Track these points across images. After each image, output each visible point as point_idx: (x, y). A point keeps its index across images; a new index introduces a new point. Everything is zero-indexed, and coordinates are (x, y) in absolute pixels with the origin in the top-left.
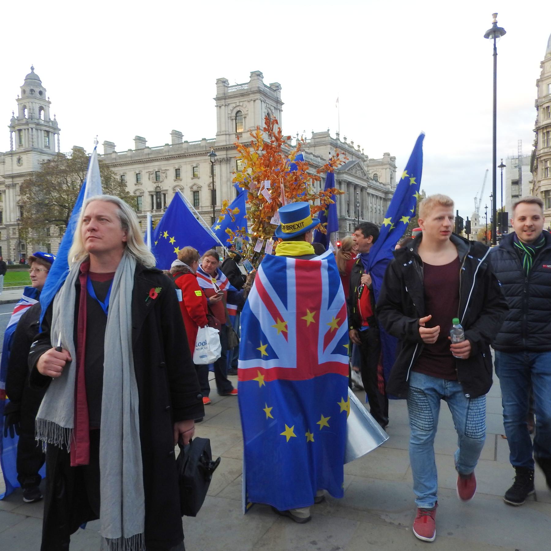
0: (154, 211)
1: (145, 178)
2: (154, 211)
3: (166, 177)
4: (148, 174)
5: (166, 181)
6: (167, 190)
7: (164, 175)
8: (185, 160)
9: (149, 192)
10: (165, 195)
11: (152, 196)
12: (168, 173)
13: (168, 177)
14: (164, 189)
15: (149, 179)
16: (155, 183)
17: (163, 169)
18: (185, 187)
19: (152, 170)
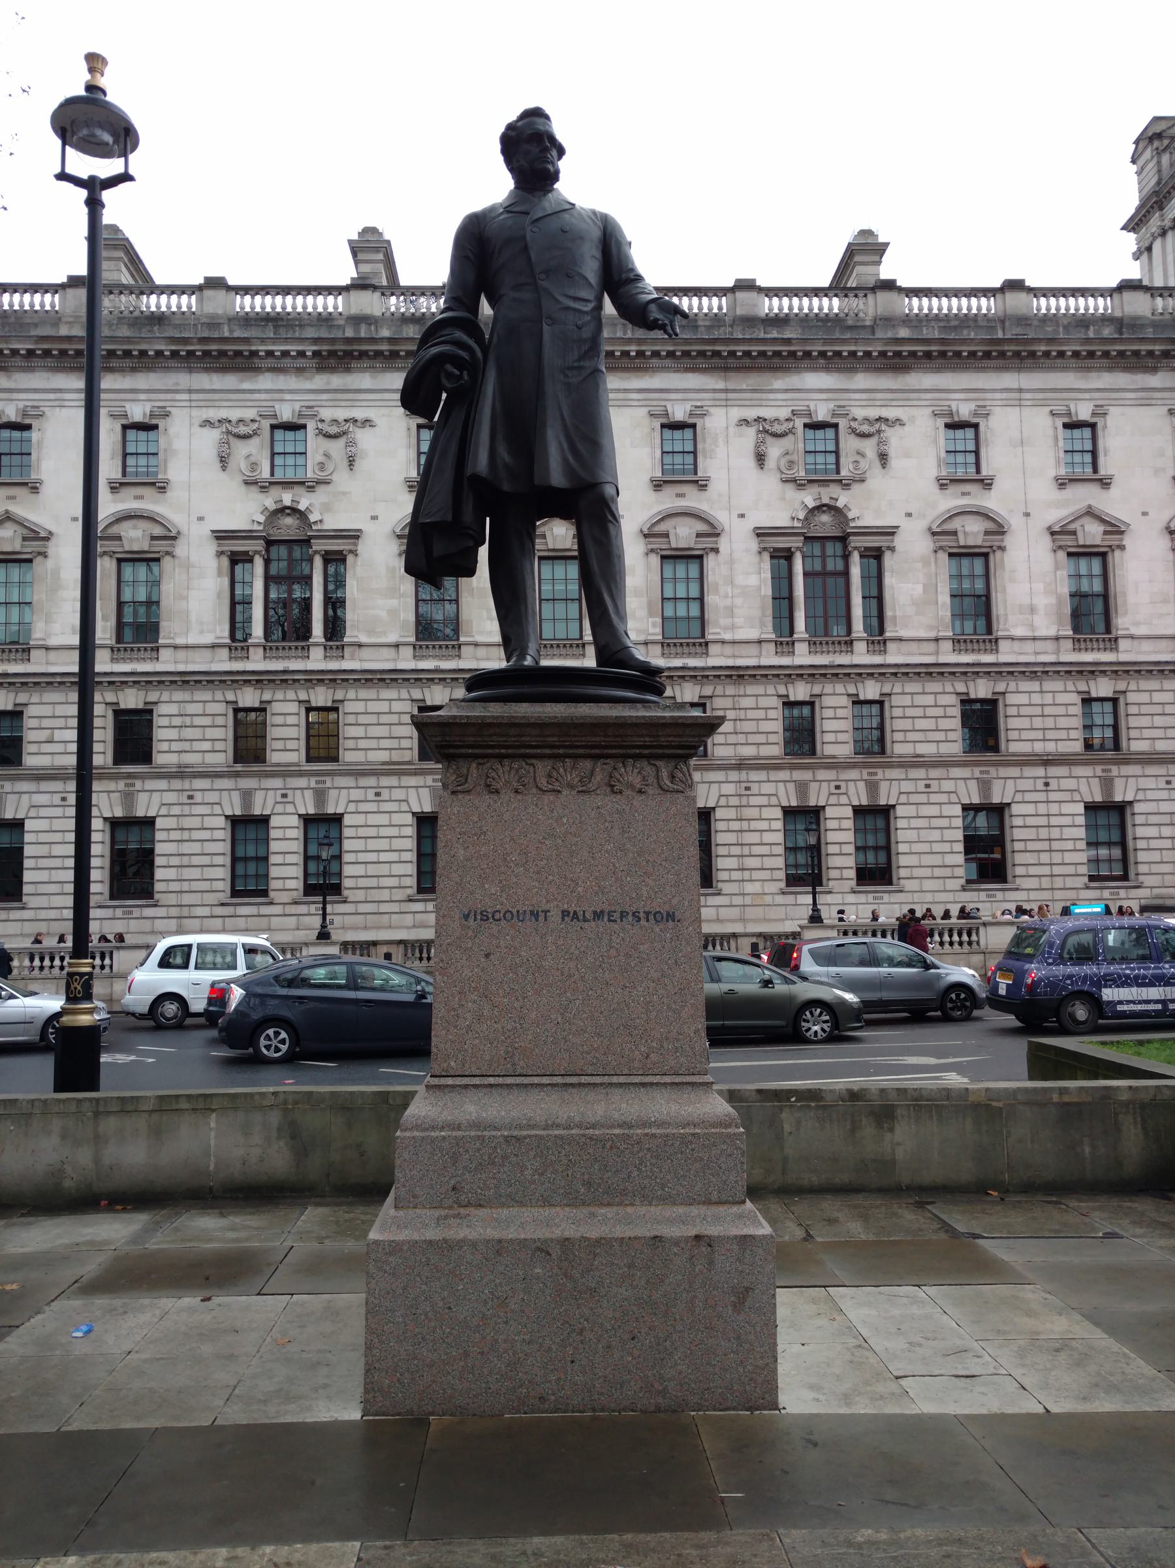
0: (801, 648)
1: (727, 452)
2: (801, 648)
3: (883, 458)
4: (751, 433)
5: (877, 480)
6: (890, 532)
7: (869, 447)
8: (1009, 380)
9: (761, 533)
10: (875, 556)
11: (782, 557)
12: (895, 439)
13: (894, 462)
14: (869, 520)
15: (760, 458)
16: (799, 484)
17: (859, 413)
18: (1015, 522)
19: (784, 413)
